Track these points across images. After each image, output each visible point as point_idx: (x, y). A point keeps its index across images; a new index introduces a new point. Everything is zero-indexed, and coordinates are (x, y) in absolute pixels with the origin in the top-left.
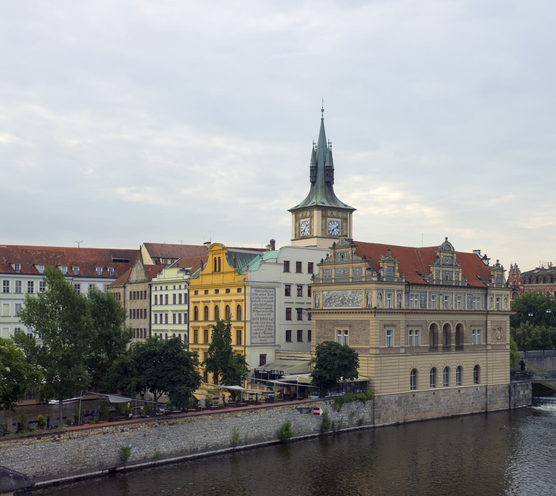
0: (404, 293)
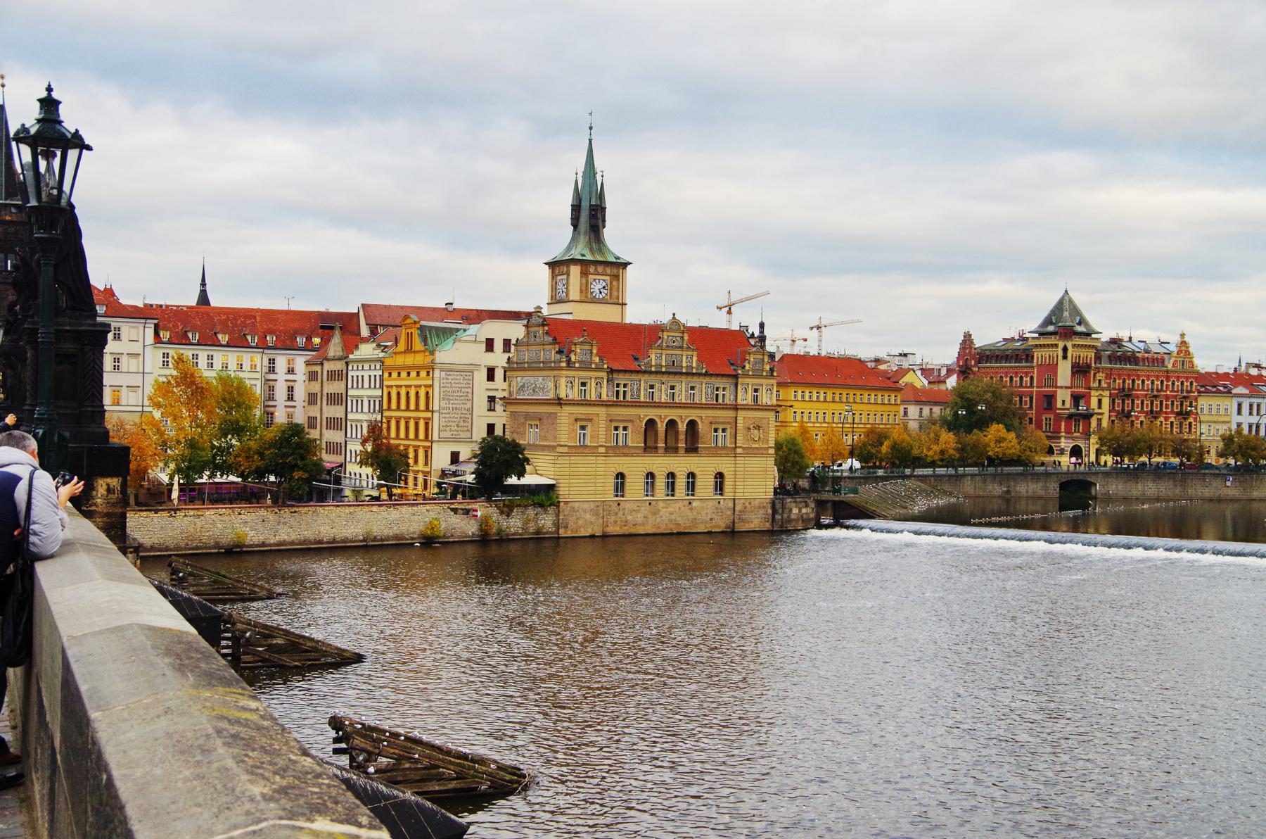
0: (605, 381)
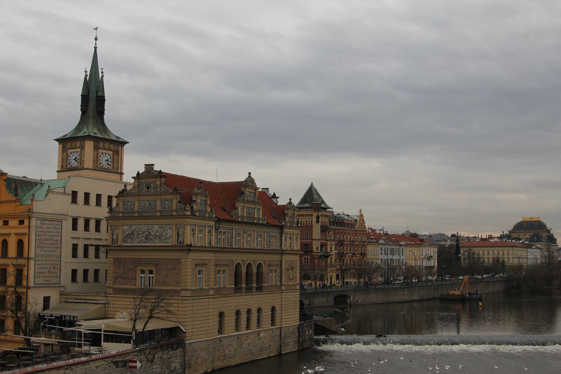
0: (214, 229)
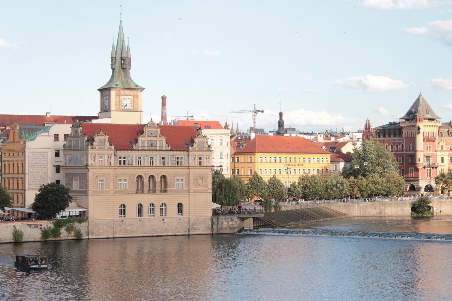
0: (113, 156)
